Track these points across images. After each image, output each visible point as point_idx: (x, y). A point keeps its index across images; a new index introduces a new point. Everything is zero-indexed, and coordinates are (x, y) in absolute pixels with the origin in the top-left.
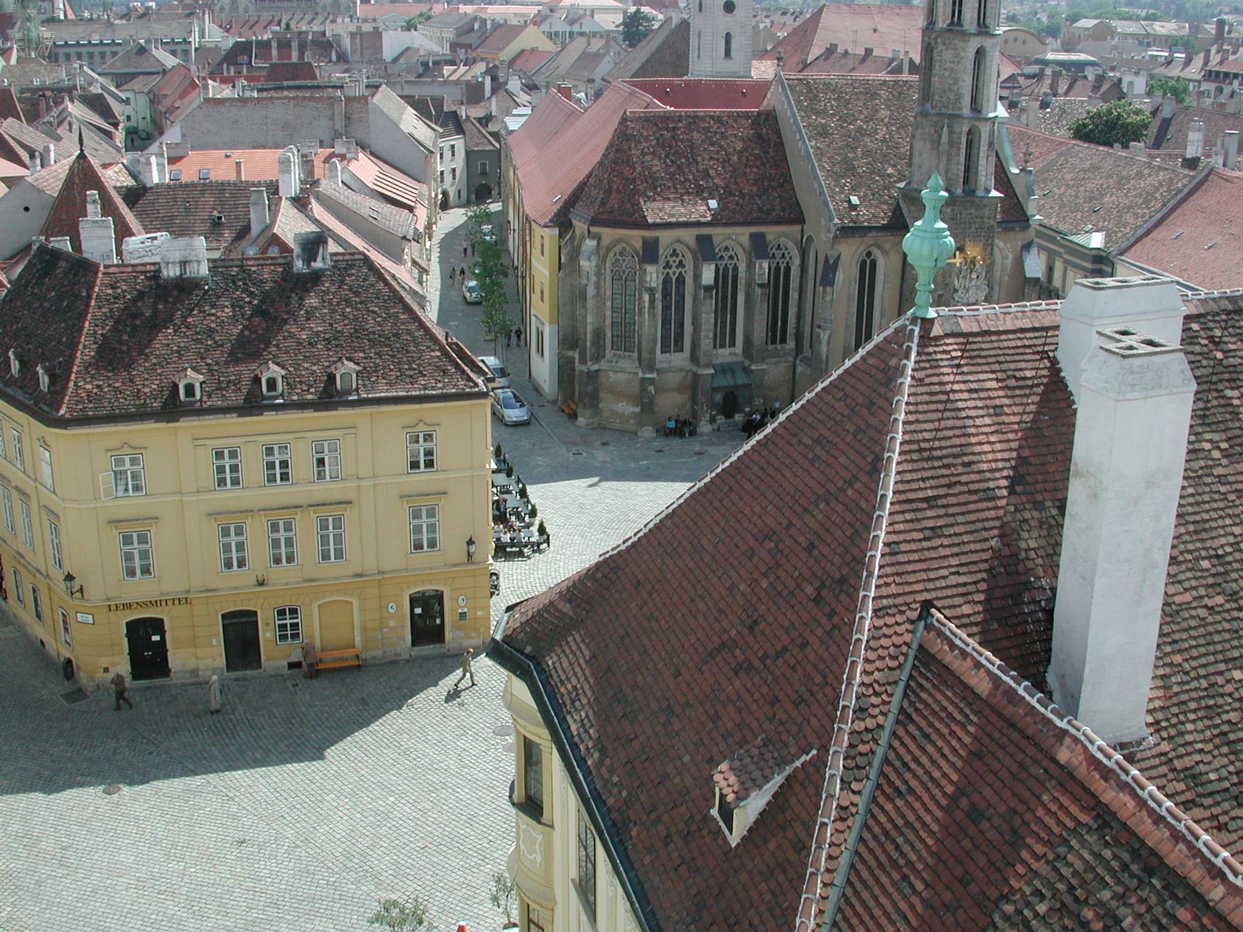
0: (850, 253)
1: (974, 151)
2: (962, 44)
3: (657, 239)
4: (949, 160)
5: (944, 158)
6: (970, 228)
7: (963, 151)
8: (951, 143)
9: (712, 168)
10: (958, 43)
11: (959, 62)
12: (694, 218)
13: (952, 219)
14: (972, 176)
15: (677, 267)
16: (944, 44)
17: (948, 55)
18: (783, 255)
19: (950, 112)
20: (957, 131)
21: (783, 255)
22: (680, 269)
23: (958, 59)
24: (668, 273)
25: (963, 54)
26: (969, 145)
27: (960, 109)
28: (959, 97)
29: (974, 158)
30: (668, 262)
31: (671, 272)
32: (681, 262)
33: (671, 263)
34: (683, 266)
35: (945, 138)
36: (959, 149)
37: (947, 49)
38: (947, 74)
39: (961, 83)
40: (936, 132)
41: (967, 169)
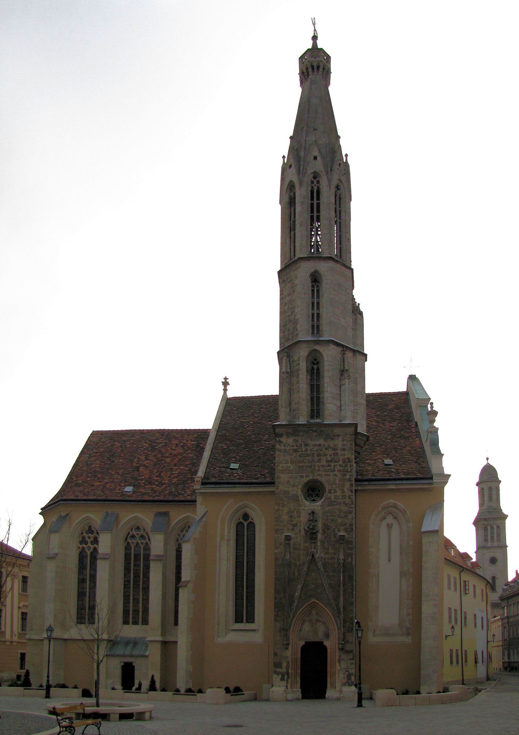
6: (319, 461)
13: (296, 451)
15: (92, 543)
24: (83, 548)
30: (83, 538)
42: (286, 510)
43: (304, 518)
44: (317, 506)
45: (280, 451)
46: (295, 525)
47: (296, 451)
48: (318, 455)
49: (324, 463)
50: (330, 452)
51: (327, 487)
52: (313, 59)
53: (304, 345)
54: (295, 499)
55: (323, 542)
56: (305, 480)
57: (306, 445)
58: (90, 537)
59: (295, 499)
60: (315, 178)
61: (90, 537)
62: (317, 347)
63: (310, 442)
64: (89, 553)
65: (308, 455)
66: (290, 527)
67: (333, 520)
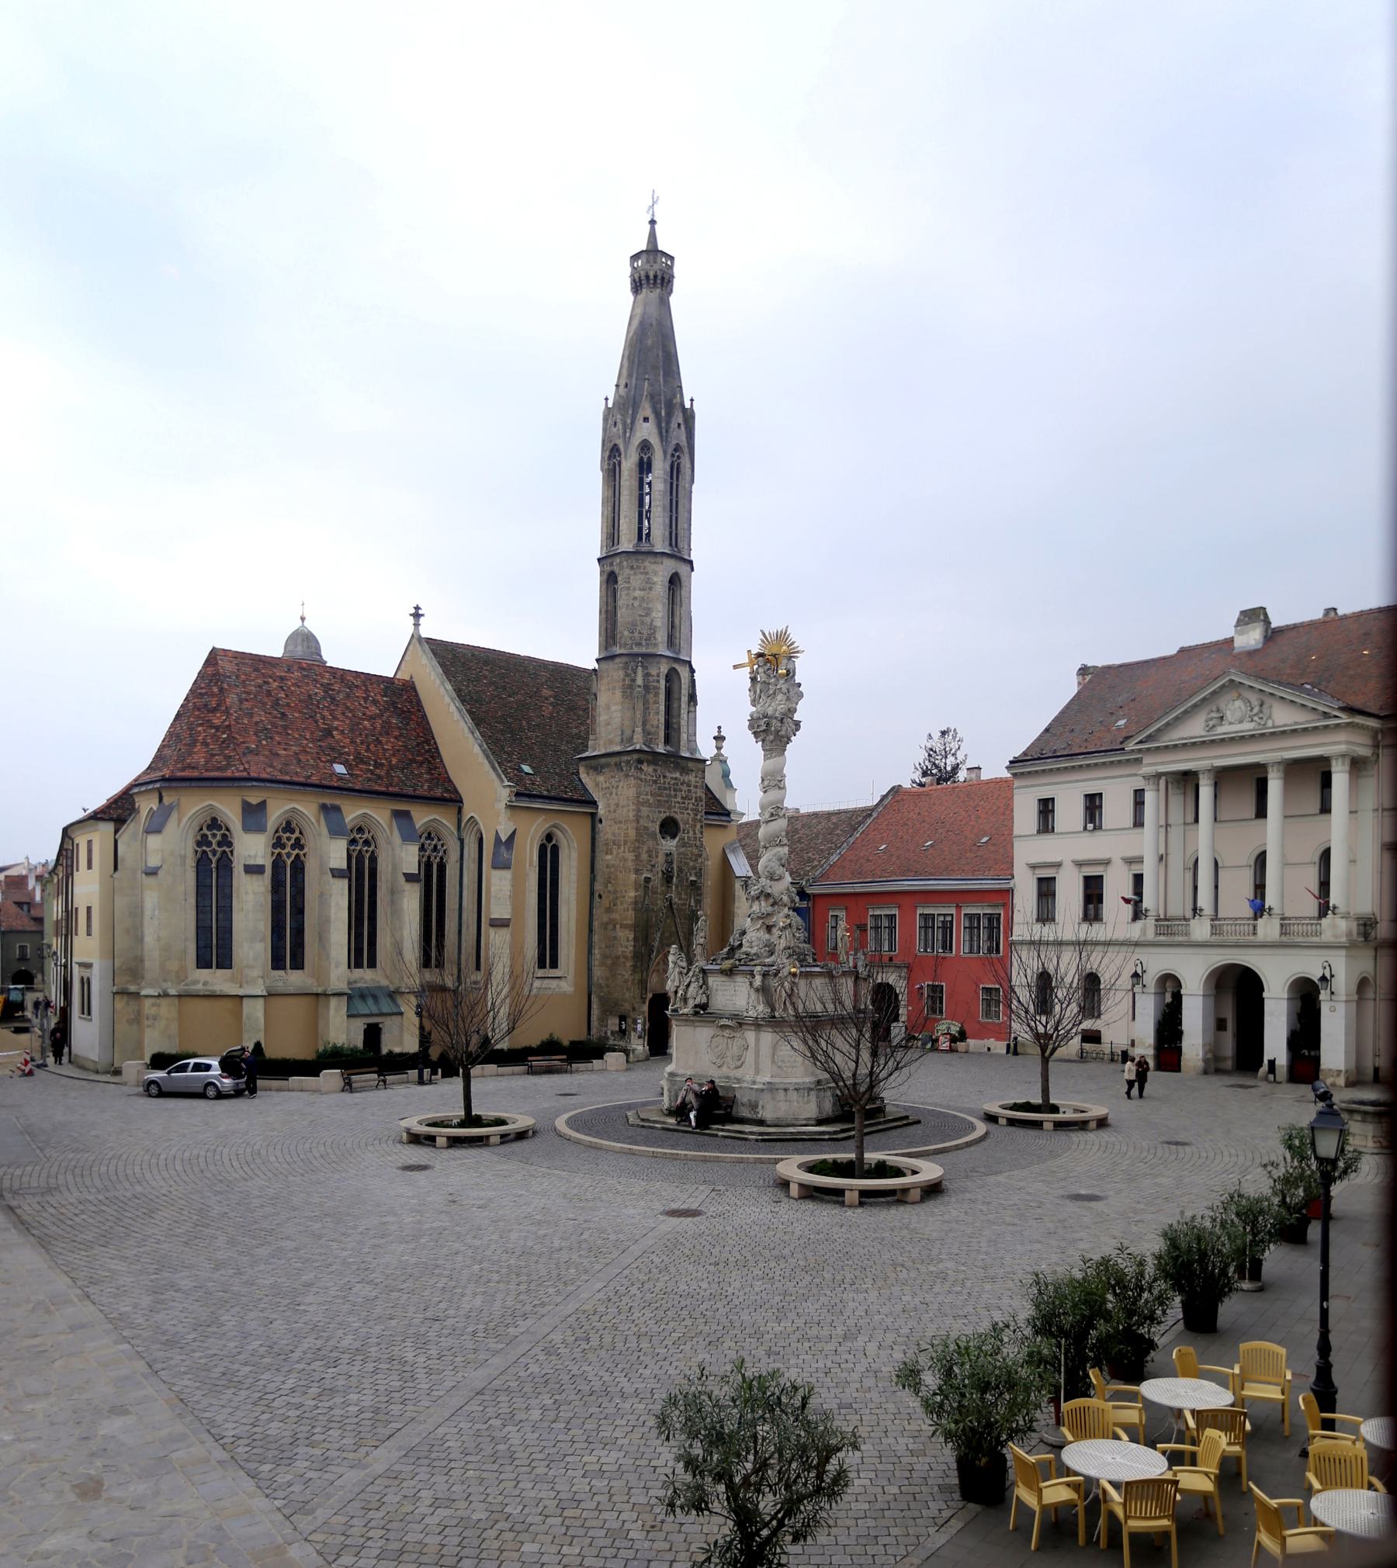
0: (531, 832)
1: (675, 705)
2: (654, 567)
3: (263, 805)
4: (646, 709)
5: (640, 705)
7: (662, 697)
8: (647, 688)
9: (337, 729)
10: (648, 564)
11: (651, 589)
12: (314, 780)
13: (655, 782)
14: (673, 734)
15: (293, 847)
16: (632, 568)
17: (637, 581)
18: (435, 846)
19: (643, 650)
20: (654, 672)
21: (435, 846)
22: (296, 851)
23: (649, 586)
24: (279, 854)
25: (655, 579)
26: (669, 693)
27: (655, 645)
28: (653, 629)
29: (674, 712)
30: (279, 838)
31: (283, 852)
32: (298, 840)
33: (284, 840)
34: (302, 847)
35: (639, 681)
36: (657, 694)
37: (635, 574)
38: (636, 604)
39: (654, 614)
40: (627, 675)
41: (668, 725)
42: (645, 849)
43: (661, 859)
44: (670, 845)
45: (641, 780)
46: (653, 866)
47: (655, 782)
48: (675, 790)
49: (679, 799)
50: (685, 788)
51: (682, 826)
52: (648, 267)
53: (664, 660)
54: (653, 836)
55: (677, 887)
56: (663, 816)
57: (664, 777)
58: (288, 839)
59: (653, 836)
60: (676, 450)
61: (288, 839)
62: (676, 666)
63: (668, 774)
64: (289, 862)
65: (665, 789)
66: (649, 867)
67: (686, 863)
